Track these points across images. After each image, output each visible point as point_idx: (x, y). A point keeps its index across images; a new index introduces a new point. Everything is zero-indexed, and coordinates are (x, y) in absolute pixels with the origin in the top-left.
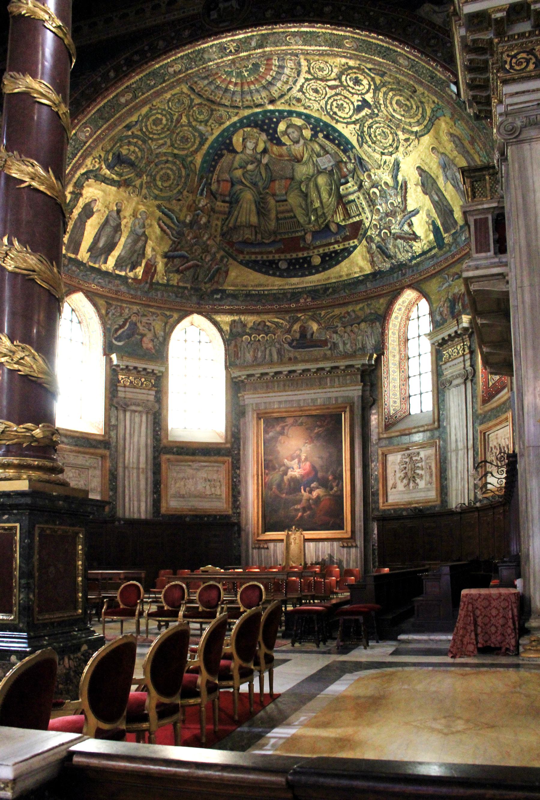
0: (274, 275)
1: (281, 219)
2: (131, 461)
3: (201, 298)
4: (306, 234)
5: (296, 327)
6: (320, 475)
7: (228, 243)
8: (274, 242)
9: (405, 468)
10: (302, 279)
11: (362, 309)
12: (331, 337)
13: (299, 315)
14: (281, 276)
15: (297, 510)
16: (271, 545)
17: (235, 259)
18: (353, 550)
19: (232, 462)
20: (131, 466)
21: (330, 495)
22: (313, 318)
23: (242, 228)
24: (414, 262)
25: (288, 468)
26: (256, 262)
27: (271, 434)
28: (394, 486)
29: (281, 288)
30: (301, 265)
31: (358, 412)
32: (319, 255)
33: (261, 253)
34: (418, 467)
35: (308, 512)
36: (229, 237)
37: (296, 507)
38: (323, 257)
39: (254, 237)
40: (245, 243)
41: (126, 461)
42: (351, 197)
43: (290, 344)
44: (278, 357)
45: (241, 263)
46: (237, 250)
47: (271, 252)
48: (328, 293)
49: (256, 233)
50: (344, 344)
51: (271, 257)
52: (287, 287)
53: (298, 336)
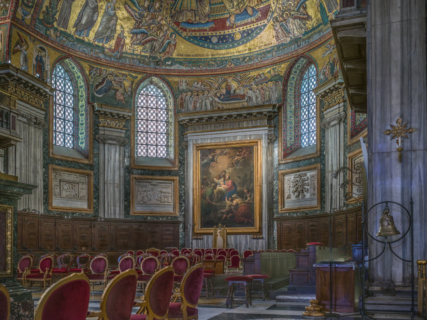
0: (208, 47)
1: (213, 5)
2: (109, 178)
4: (230, 16)
6: (239, 188)
7: (175, 23)
9: (297, 184)
10: (228, 50)
12: (247, 93)
13: (226, 77)
15: (223, 213)
16: (205, 237)
17: (180, 36)
18: (260, 241)
19: (179, 181)
20: (109, 182)
21: (245, 203)
22: (234, 80)
23: (185, 11)
25: (216, 184)
26: (195, 38)
27: (205, 161)
28: (289, 197)
29: (213, 57)
32: (240, 32)
33: (199, 31)
34: (305, 183)
35: (230, 214)
36: (176, 18)
37: (222, 211)
39: (194, 19)
40: (188, 23)
41: (106, 179)
43: (219, 98)
44: (211, 107)
45: (185, 38)
46: (181, 28)
47: (206, 30)
48: (246, 60)
49: (195, 14)
50: (257, 98)
51: (206, 35)
52: (217, 56)
53: (224, 91)
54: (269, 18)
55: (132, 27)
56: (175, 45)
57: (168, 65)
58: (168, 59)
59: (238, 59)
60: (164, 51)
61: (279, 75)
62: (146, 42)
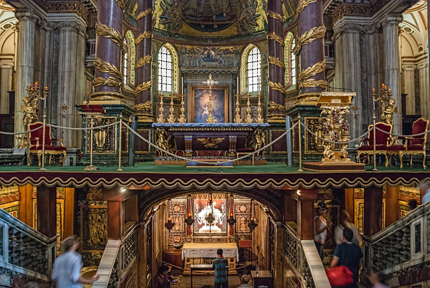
0: (199, 30)
3: (170, 36)
5: (206, 53)
7: (183, 15)
8: (201, 17)
11: (232, 49)
14: (201, 31)
17: (185, 22)
22: (212, 49)
24: (254, 34)
30: (210, 28)
31: (230, 89)
38: (219, 26)
40: (190, 15)
42: (234, 5)
43: (203, 59)
45: (187, 23)
46: (186, 18)
47: (199, 21)
50: (225, 62)
53: (206, 56)
54: (234, 20)
55: (161, 15)
56: (181, 27)
57: (176, 37)
58: (176, 34)
59: (215, 39)
60: (175, 29)
61: (238, 51)
62: (167, 23)
